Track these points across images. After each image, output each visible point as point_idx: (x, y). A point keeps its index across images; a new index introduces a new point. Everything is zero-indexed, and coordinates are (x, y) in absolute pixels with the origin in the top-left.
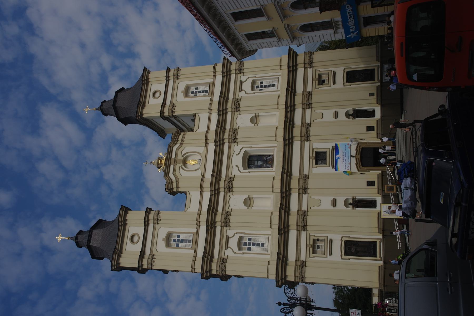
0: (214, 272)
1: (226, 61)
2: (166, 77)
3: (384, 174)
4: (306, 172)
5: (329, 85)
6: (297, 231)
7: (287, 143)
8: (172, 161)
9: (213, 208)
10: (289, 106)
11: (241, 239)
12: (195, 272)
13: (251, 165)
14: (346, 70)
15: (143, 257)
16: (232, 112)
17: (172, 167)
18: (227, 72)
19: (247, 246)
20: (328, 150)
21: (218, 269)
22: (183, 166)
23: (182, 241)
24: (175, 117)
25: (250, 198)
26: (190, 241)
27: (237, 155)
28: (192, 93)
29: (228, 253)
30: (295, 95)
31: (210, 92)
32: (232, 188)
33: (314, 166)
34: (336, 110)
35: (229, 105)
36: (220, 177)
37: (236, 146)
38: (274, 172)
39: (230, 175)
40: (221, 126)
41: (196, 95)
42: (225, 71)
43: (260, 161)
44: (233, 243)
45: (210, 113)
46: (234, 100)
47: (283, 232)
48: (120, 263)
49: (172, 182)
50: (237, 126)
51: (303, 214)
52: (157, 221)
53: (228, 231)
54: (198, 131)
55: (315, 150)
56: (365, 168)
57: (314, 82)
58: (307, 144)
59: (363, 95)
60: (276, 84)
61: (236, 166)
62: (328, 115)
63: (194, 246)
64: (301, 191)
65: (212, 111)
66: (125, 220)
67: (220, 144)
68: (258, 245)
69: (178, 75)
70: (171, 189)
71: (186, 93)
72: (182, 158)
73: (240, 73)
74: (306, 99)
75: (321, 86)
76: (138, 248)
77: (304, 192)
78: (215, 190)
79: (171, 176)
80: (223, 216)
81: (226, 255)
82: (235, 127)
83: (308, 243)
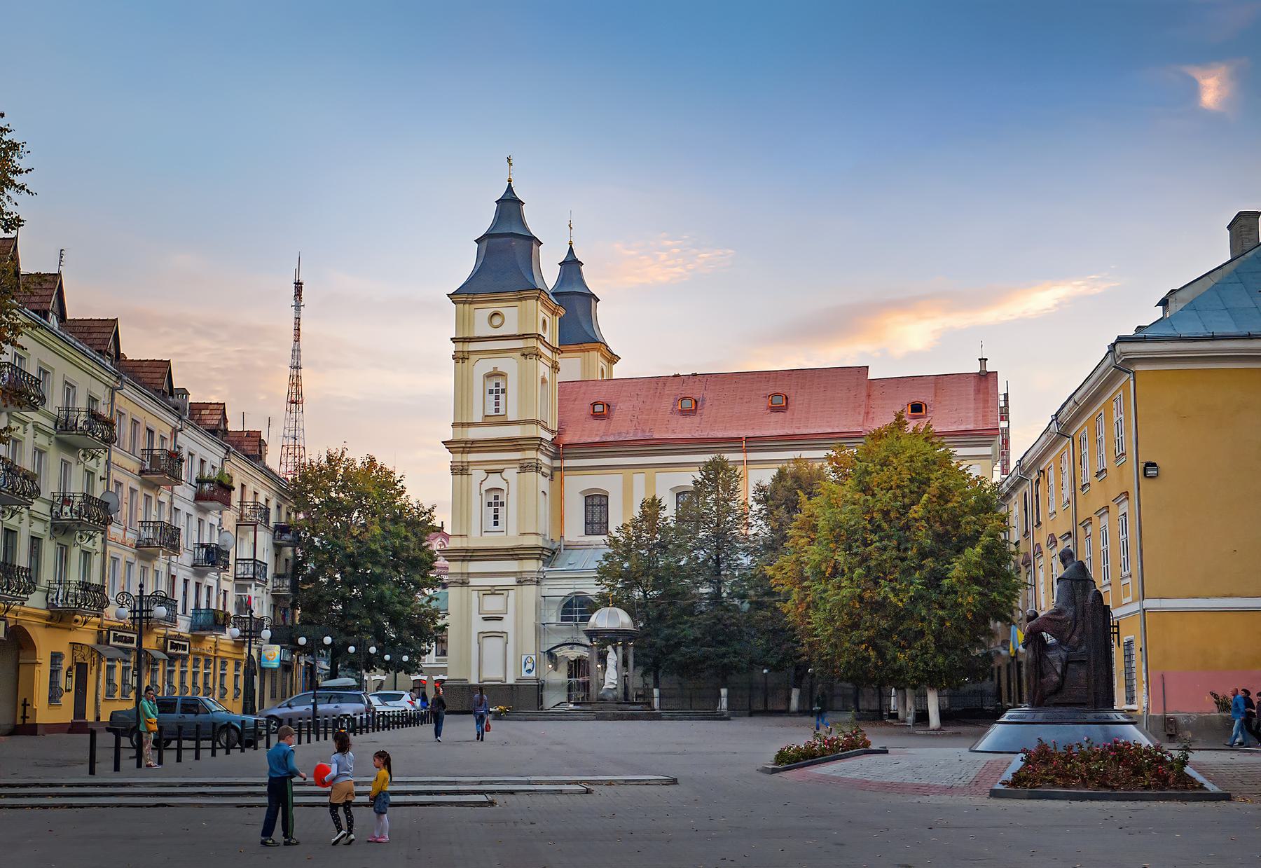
23: (497, 398)
26: (497, 410)
44: (494, 481)
63: (488, 419)
68: (496, 517)
76: (482, 329)
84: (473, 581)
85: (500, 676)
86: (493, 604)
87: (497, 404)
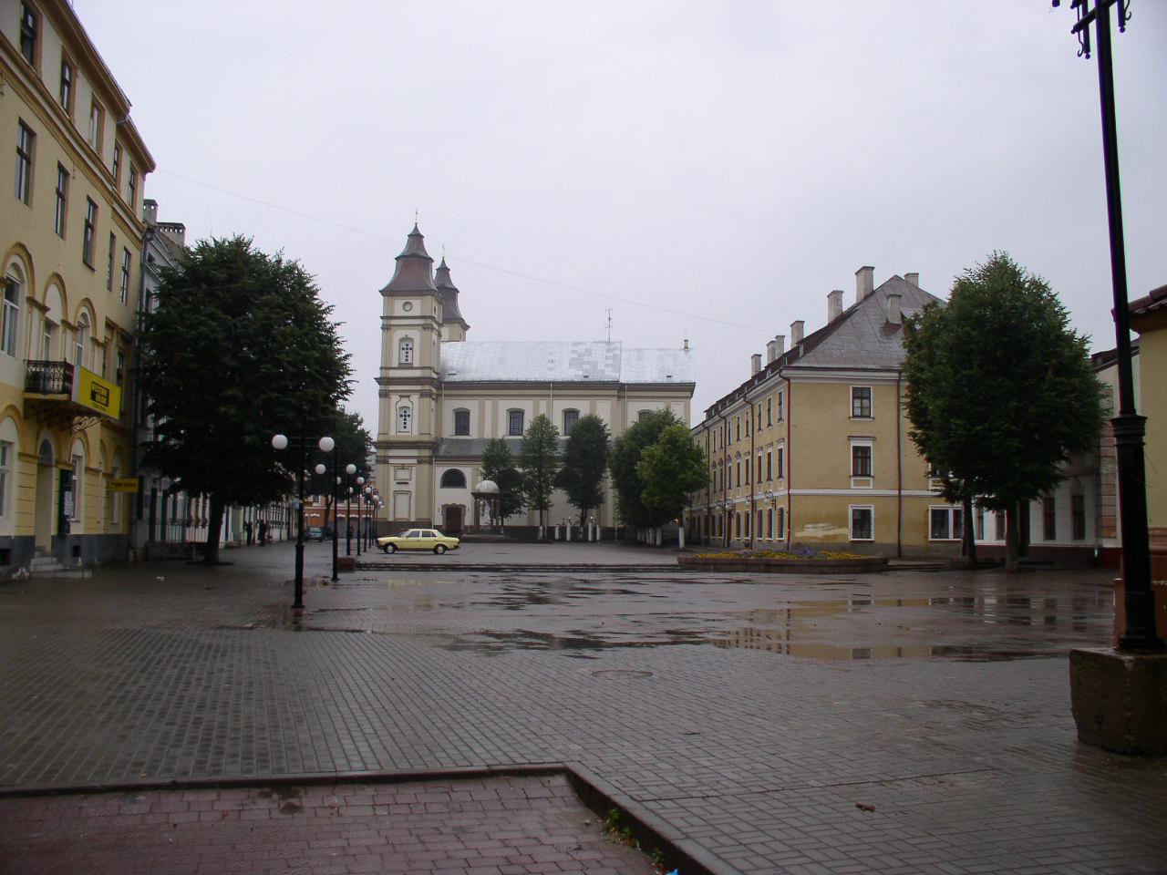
23: (407, 353)
63: (402, 366)
68: (405, 423)
84: (391, 461)
85: (406, 516)
86: (403, 475)
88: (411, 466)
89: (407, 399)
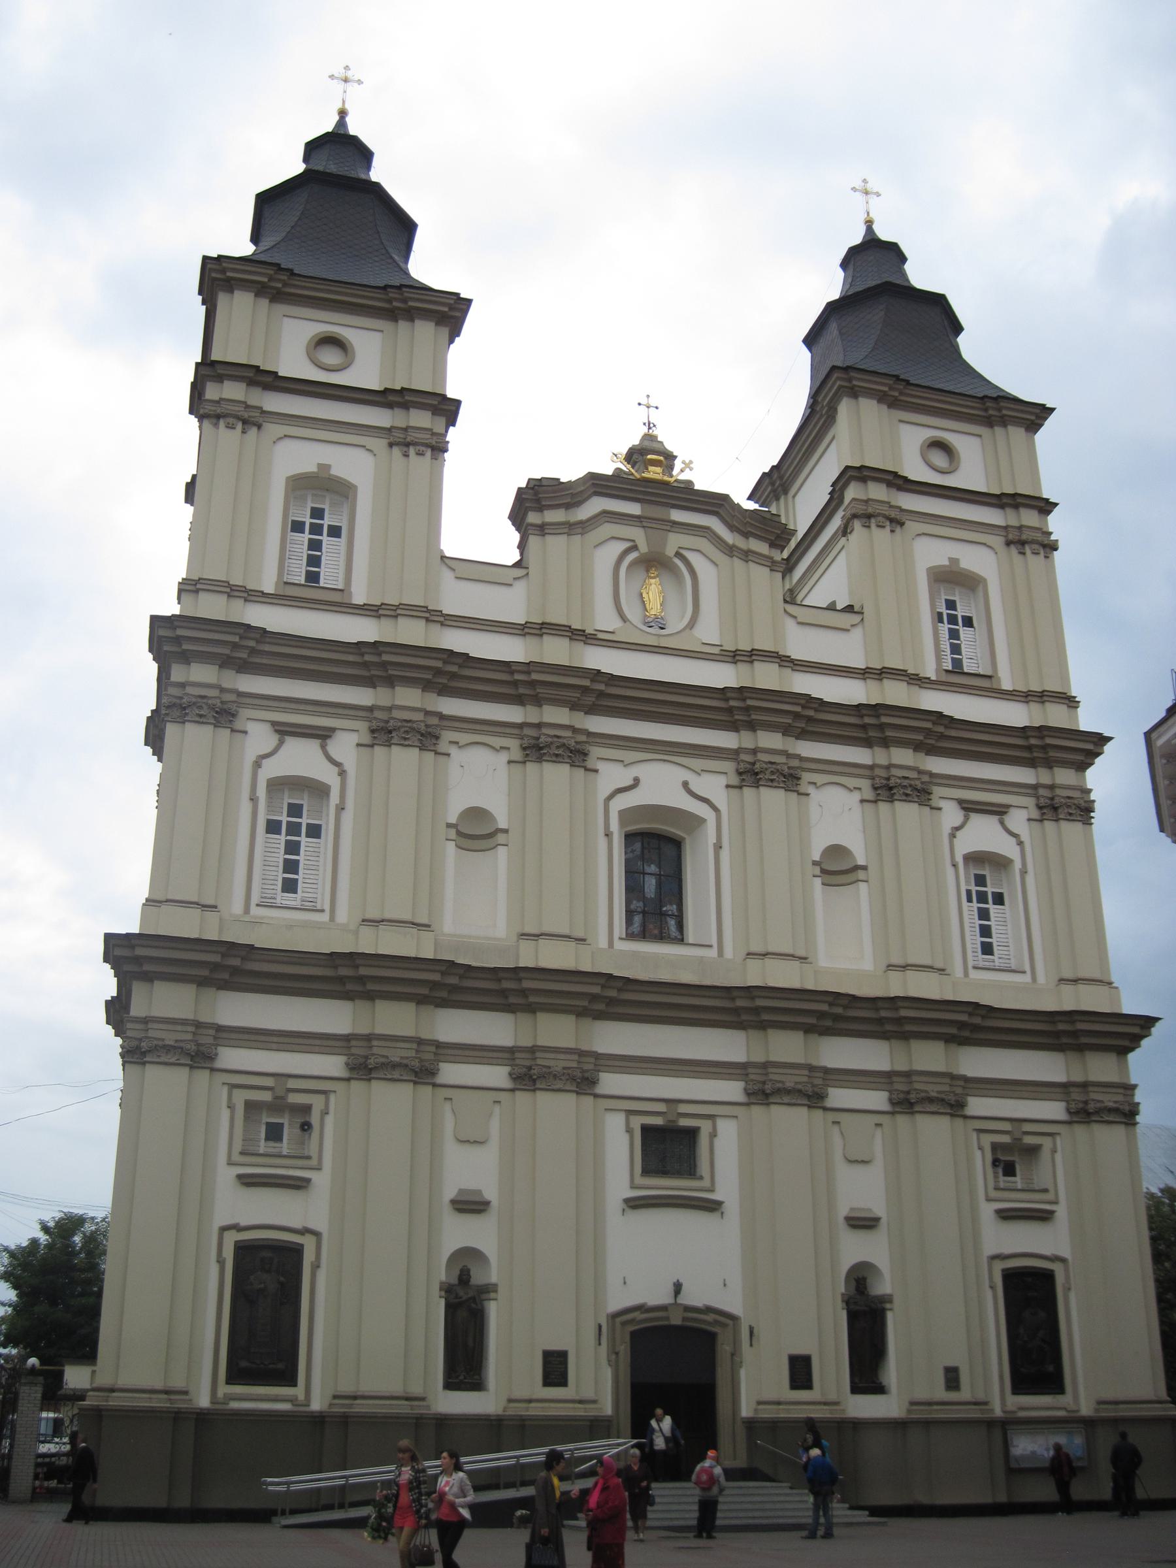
0: (178, 673)
1: (1090, 747)
2: (1015, 496)
3: (597, 1428)
4: (611, 1082)
5: (993, 1194)
6: (347, 1038)
7: (740, 1003)
8: (656, 512)
9: (453, 676)
10: (904, 1013)
11: (319, 790)
12: (180, 591)
13: (638, 846)
14: (1057, 1268)
15: (251, 383)
16: (871, 767)
17: (634, 509)
18: (1045, 748)
19: (284, 819)
20: (706, 1183)
21: (189, 690)
22: (633, 556)
23: (315, 545)
24: (845, 531)
25: (491, 835)
26: (313, 577)
27: (685, 785)
28: (951, 605)
29: (259, 737)
30: (949, 1039)
31: (957, 678)
32: (540, 760)
33: (637, 1122)
34: (884, 1221)
35: (903, 756)
36: (591, 710)
37: (722, 781)
38: (611, 944)
39: (596, 751)
40: (810, 719)
41: (941, 621)
42: (1049, 741)
43: (659, 885)
45: (864, 674)
46: (926, 778)
47: (344, 972)
48: (231, 291)
49: (568, 506)
50: (811, 790)
51: (421, 1066)
52: (402, 441)
53: (353, 738)
54: (790, 624)
55: (705, 1127)
56: (624, 1349)
57: (1007, 1126)
58: (732, 1090)
59: (947, 1341)
60: (996, 959)
61: (636, 782)
62: (863, 1189)
63: (291, 591)
64: (523, 1060)
65: (872, 684)
66: (411, 315)
67: (730, 710)
68: (291, 867)
69: (1023, 543)
70: (538, 501)
71: (950, 578)
72: (670, 551)
73: (1040, 808)
74: (933, 1090)
75: (989, 1157)
76: (293, 362)
77: (517, 1070)
78: (533, 684)
79: (596, 505)
80: (419, 716)
81: (251, 727)
82: (806, 777)
83: (292, 1084)
87: (314, 561)
88: (321, 1086)
89: (313, 746)
